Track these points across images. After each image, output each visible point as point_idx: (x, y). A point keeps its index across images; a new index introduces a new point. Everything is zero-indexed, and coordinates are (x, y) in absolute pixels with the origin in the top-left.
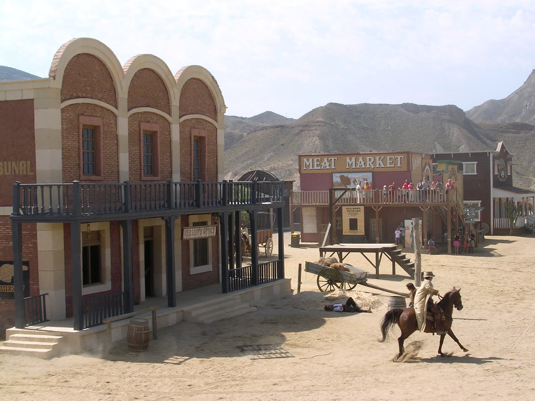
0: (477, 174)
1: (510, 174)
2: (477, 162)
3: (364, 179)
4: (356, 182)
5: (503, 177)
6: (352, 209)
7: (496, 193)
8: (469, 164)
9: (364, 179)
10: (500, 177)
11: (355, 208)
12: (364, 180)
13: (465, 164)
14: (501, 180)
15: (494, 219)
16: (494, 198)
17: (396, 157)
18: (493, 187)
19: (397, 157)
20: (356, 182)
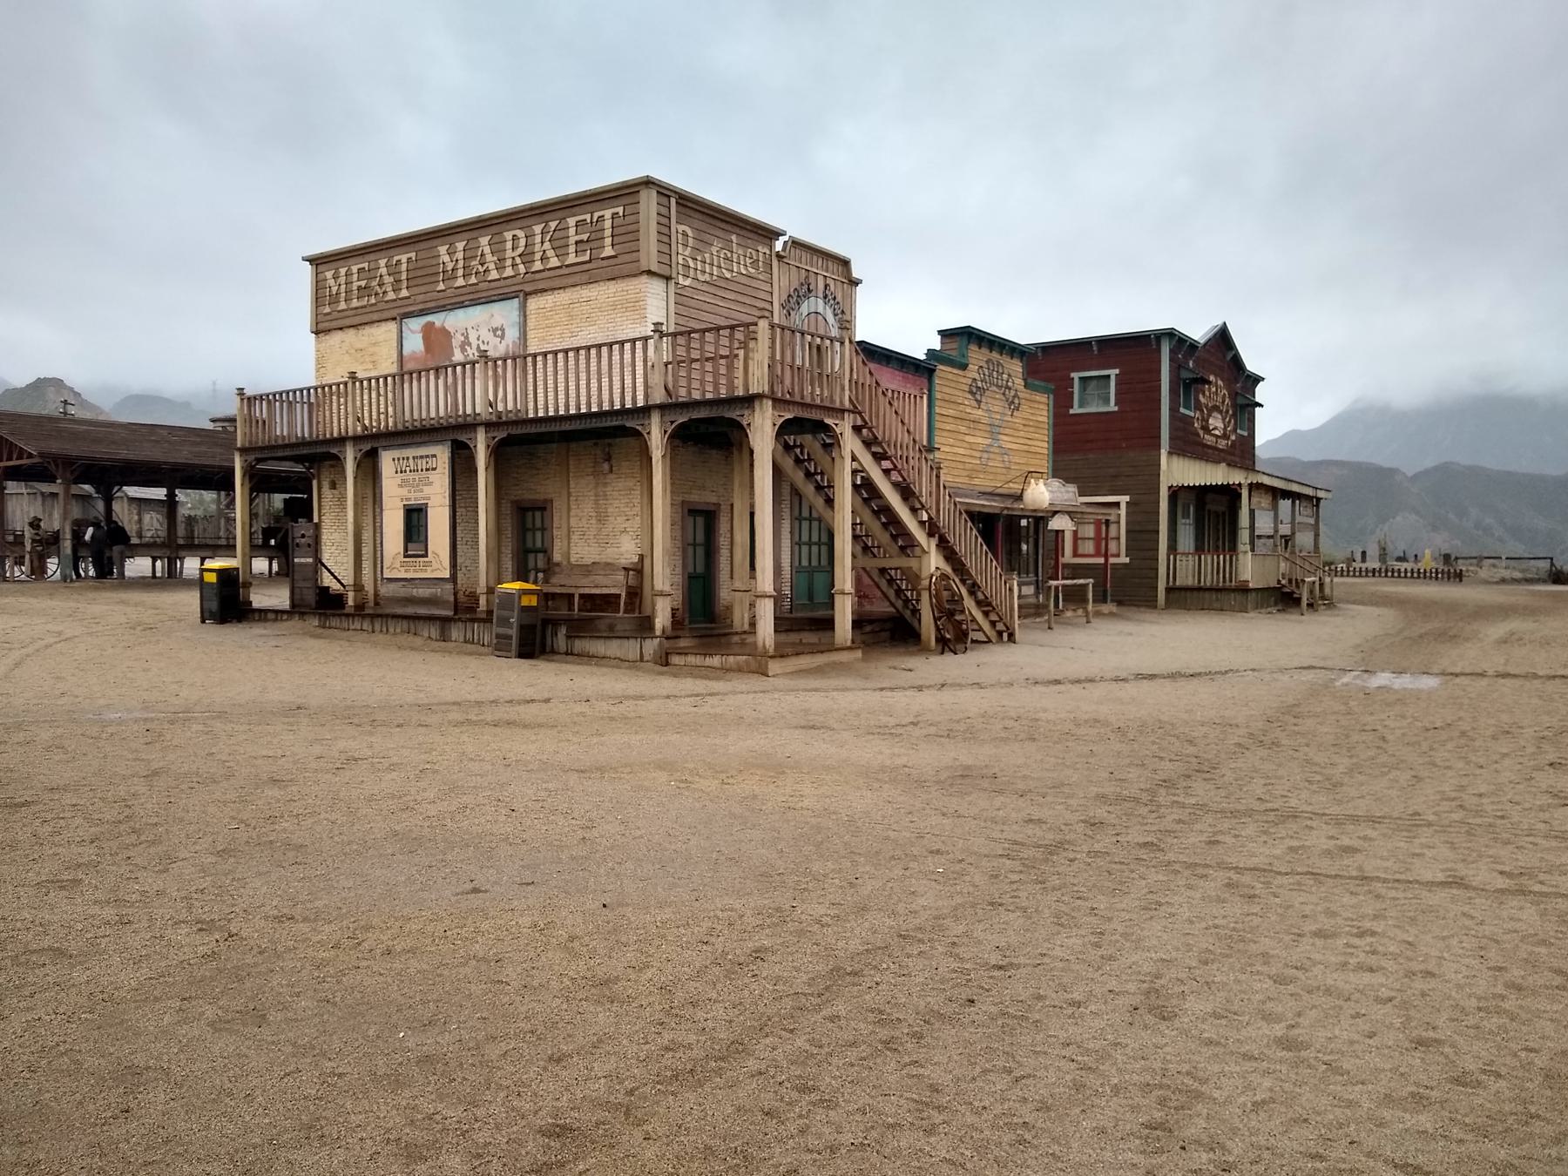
0: (1116, 409)
1: (1246, 434)
2: (1117, 371)
3: (495, 330)
4: (468, 348)
5: (1217, 432)
6: (411, 460)
7: (1179, 472)
8: (1091, 378)
9: (495, 330)
10: (1206, 429)
11: (422, 457)
12: (495, 335)
13: (1080, 378)
14: (1209, 440)
15: (1168, 560)
16: (1170, 488)
17: (596, 215)
18: (1170, 453)
19: (601, 213)
20: (470, 345)
